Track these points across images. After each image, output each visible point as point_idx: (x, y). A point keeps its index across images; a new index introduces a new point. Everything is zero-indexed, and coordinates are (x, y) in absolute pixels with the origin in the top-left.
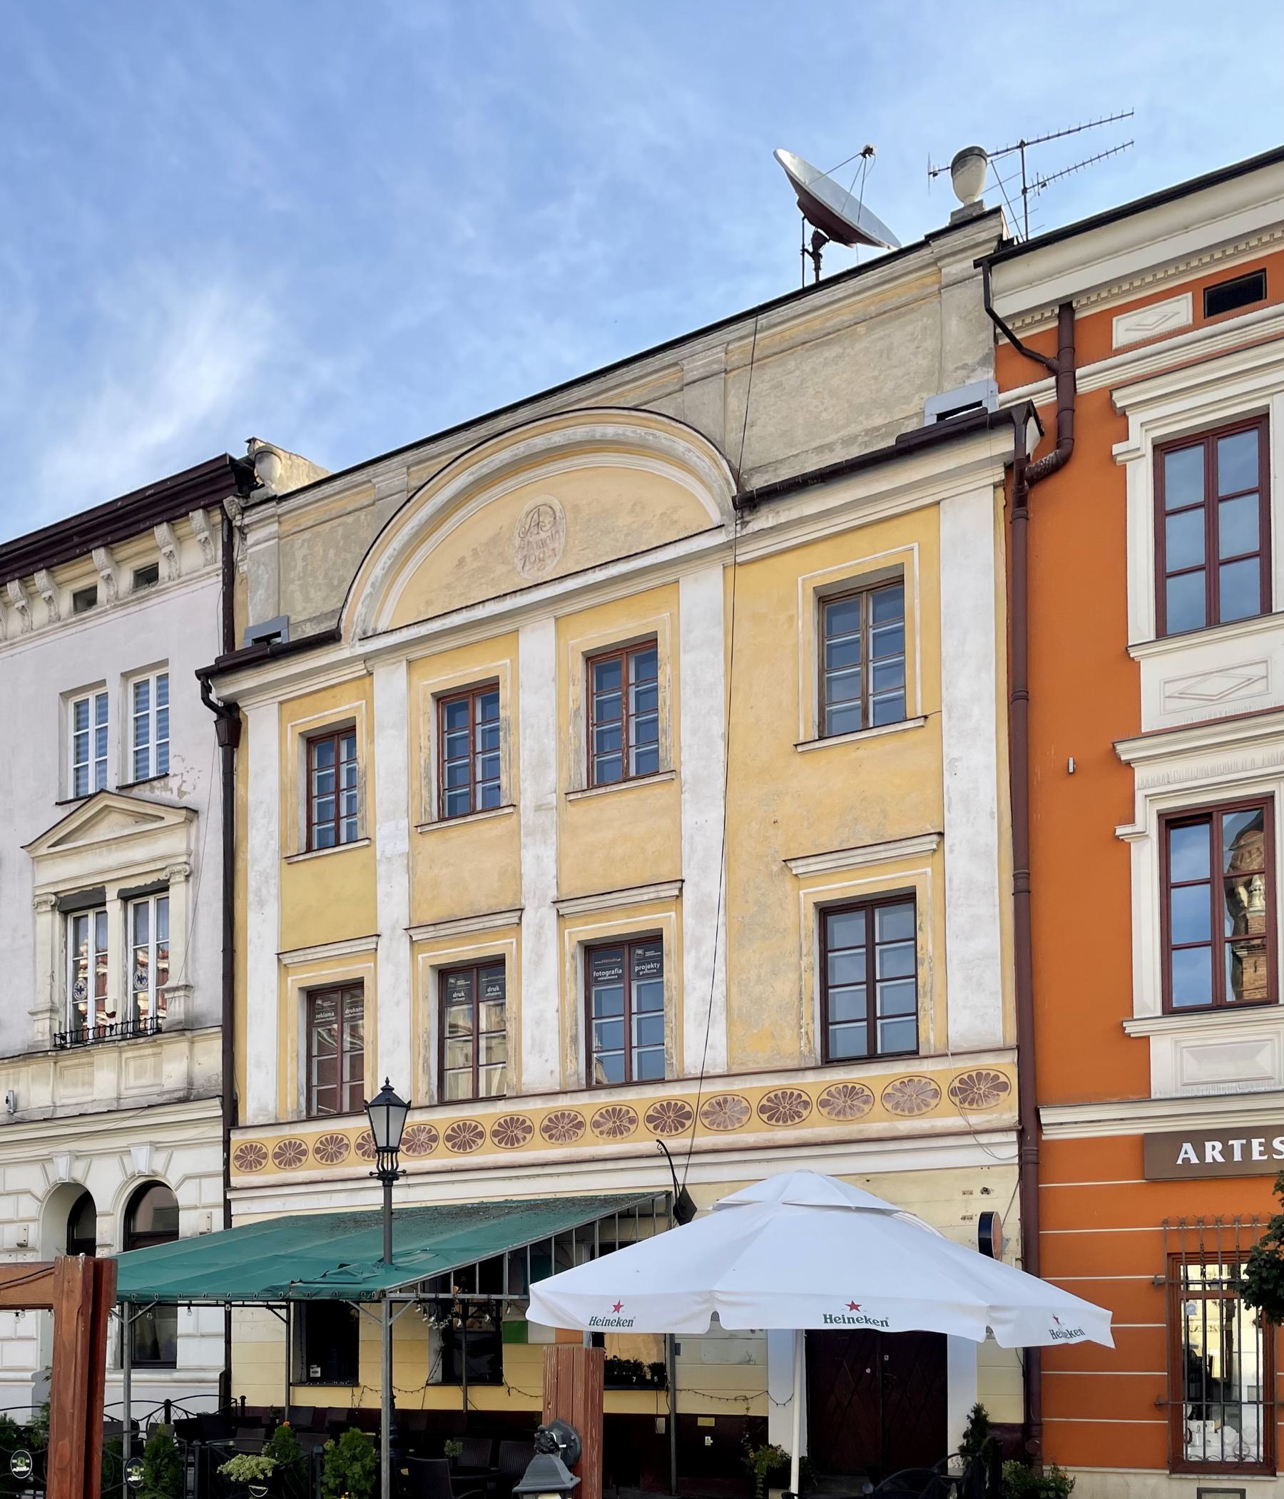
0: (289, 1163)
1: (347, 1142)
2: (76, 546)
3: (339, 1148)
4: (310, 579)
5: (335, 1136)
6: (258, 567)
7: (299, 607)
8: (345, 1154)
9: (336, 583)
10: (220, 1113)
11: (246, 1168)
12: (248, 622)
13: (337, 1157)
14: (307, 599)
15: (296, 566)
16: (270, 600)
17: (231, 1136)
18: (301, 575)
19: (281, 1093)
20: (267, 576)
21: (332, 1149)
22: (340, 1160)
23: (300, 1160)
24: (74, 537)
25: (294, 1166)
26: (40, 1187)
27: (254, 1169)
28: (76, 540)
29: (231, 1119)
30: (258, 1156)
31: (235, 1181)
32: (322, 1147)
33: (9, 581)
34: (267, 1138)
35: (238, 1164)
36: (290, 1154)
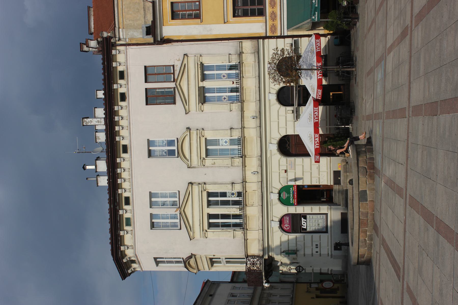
3: (273, 1)
6: (128, 35)
9: (137, 10)
10: (262, 40)
11: (276, 30)
12: (141, 37)
13: (275, 2)
18: (133, 21)
19: (259, 22)
20: (131, 32)
21: (273, 3)
23: (275, 13)
27: (276, 28)
29: (264, 38)
31: (279, 34)
32: (272, 6)
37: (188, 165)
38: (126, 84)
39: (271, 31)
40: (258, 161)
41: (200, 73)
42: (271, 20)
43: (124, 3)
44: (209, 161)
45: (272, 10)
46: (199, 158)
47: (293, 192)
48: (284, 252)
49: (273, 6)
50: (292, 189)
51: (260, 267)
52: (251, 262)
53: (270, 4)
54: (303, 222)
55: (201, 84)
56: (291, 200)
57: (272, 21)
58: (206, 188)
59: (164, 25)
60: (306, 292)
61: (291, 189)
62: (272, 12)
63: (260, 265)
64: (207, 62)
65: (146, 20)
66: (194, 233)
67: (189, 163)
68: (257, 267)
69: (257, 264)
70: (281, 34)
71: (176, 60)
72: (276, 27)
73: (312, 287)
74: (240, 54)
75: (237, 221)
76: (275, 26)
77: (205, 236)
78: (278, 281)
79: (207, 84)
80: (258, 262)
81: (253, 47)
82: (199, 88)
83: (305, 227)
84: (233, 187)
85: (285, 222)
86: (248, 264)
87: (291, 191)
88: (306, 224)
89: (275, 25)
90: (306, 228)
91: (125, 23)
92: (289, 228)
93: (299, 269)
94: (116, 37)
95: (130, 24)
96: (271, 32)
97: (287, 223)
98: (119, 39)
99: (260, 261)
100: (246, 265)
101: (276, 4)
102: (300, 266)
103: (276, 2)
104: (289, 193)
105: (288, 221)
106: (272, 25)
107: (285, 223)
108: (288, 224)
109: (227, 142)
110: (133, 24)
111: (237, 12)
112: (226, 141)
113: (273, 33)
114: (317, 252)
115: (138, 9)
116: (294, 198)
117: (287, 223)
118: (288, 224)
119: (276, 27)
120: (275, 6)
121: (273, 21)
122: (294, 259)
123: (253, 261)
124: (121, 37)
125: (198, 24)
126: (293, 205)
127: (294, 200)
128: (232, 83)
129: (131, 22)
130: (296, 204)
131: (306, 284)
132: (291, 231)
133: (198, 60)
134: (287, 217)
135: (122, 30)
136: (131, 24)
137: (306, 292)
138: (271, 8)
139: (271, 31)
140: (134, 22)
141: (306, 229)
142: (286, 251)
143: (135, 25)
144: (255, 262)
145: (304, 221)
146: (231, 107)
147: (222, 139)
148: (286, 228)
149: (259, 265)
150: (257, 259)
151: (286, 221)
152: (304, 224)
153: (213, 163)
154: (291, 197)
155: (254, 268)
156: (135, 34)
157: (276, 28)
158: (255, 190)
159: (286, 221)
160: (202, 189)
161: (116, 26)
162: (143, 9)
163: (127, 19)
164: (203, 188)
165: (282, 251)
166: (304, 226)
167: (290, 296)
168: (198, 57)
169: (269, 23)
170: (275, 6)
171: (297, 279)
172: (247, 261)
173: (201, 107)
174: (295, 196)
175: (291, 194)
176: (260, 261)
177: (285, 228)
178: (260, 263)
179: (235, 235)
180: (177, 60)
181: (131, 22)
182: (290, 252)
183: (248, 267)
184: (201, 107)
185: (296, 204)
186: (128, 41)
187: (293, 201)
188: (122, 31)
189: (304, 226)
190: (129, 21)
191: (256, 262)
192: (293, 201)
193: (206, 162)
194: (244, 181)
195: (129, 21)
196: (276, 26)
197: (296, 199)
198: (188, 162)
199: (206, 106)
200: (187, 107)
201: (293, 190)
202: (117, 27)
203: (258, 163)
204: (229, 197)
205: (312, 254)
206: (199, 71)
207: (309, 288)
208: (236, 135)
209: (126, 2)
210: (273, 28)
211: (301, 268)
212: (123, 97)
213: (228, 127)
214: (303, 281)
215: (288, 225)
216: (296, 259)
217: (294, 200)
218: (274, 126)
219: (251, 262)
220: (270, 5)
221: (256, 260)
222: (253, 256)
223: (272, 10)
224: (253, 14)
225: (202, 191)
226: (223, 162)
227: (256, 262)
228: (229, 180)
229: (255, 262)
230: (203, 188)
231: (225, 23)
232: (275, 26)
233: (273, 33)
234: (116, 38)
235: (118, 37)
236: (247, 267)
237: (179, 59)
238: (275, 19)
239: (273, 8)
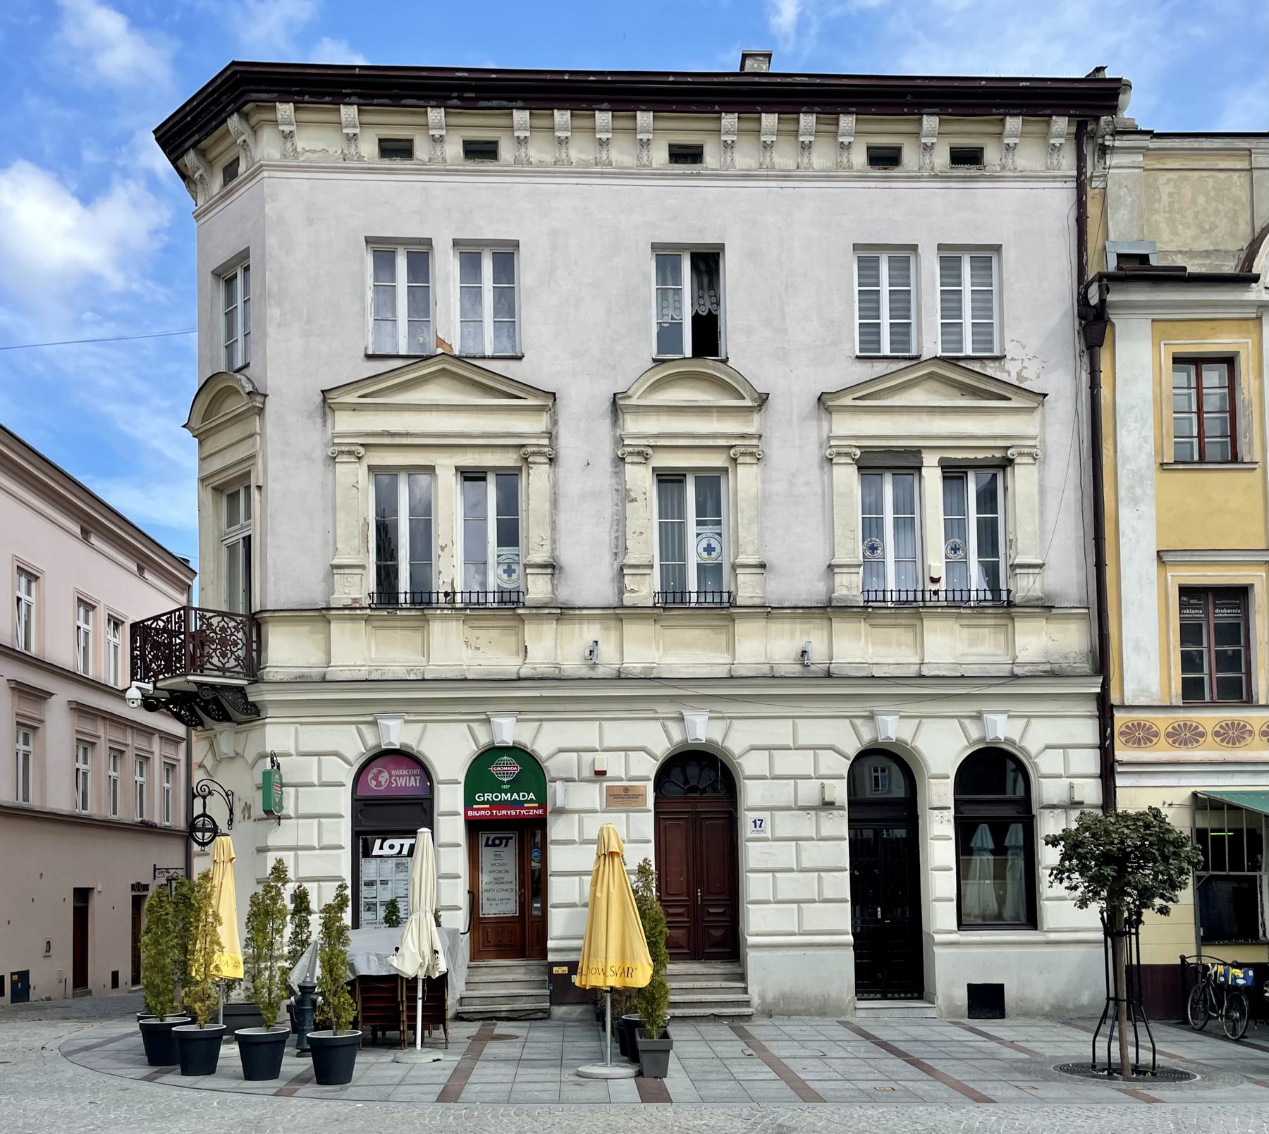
0: (1185, 743)
1: (1251, 729)
2: (906, 105)
4: (1177, 216)
5: (1236, 722)
7: (1166, 236)
8: (1249, 739)
9: (1207, 227)
11: (1134, 743)
13: (1239, 741)
14: (1174, 232)
15: (1161, 198)
16: (1135, 223)
17: (1115, 713)
18: (1167, 209)
20: (1130, 199)
21: (1233, 733)
22: (1243, 744)
23: (1197, 741)
24: (910, 96)
25: (1190, 746)
26: (853, 747)
27: (1143, 745)
28: (909, 98)
30: (1148, 734)
32: (1222, 731)
33: (804, 113)
34: (1157, 718)
35: (1124, 740)
36: (1186, 735)
37: (625, 395)
38: (933, 169)
39: (1133, 724)
40: (643, 667)
41: (971, 455)
42: (1173, 728)
43: (1235, 175)
44: (641, 478)
45: (1209, 731)
46: (652, 442)
47: (518, 804)
48: (272, 767)
49: (1225, 734)
50: (531, 801)
53: (1229, 723)
54: (397, 842)
55: (930, 461)
56: (488, 796)
57: (1170, 729)
58: (534, 463)
59: (1154, 323)
61: (532, 796)
62: (1201, 729)
63: (218, 669)
64: (1022, 480)
65: (1174, 257)
66: (354, 408)
67: (634, 401)
69: (224, 655)
70: (1122, 764)
71: (1025, 367)
72: (1146, 743)
74: (1045, 607)
75: (404, 584)
76: (1151, 741)
77: (342, 452)
79: (932, 478)
80: (232, 663)
81: (1066, 658)
82: (917, 452)
83: (376, 851)
84: (540, 571)
85: (400, 772)
87: (524, 796)
88: (392, 856)
89: (1155, 740)
90: (374, 853)
91: (1163, 177)
92: (373, 786)
93: (204, 830)
94: (1117, 137)
95: (1157, 196)
96: (1127, 727)
97: (395, 780)
98: (1104, 150)
100: (220, 613)
101: (1230, 745)
103: (1237, 745)
104: (516, 785)
105: (402, 782)
106: (1155, 729)
107: (393, 772)
108: (391, 783)
109: (709, 554)
110: (1156, 205)
111: (1192, 601)
112: (714, 549)
113: (1122, 733)
115: (1211, 230)
116: (494, 805)
117: (395, 780)
118: (391, 783)
119: (1146, 743)
120: (1222, 741)
121: (1168, 735)
122: (247, 808)
123: (236, 644)
124: (1113, 160)
125: (1160, 451)
126: (469, 802)
127: (488, 806)
128: (936, 576)
129: (1165, 199)
130: (470, 813)
132: (362, 793)
133: (1022, 450)
134: (418, 778)
135: (1140, 162)
136: (1159, 201)
138: (1218, 728)
139: (1133, 724)
140: (1164, 212)
141: (367, 853)
142: (281, 776)
143: (1155, 217)
144: (231, 651)
145: (402, 846)
146: (845, 570)
147: (720, 535)
148: (376, 778)
149: (220, 665)
151: (403, 776)
152: (392, 847)
153: (633, 495)
154: (497, 797)
156: (1122, 212)
157: (1143, 745)
158: (529, 655)
159: (403, 776)
160: (530, 449)
161: (1155, 140)
162: (1211, 248)
163: (1175, 186)
164: (534, 454)
165: (280, 760)
166: (381, 848)
168: (1035, 450)
169: (1162, 721)
170: (1224, 744)
172: (239, 619)
173: (847, 454)
174: (504, 812)
175: (509, 794)
177: (375, 771)
178: (228, 670)
179: (347, 571)
180: (1021, 371)
181: (1165, 199)
182: (276, 789)
184: (847, 454)
185: (470, 813)
186: (1094, 185)
187: (483, 803)
188: (1134, 162)
189: (381, 848)
190: (1171, 195)
191: (232, 653)
192: (483, 803)
193: (636, 467)
194: (563, 612)
195: (1171, 195)
196: (1149, 744)
197: (492, 813)
198: (637, 396)
199: (847, 477)
200: (847, 401)
201: (527, 802)
202: (1151, 145)
203: (634, 668)
204: (499, 556)
206: (981, 455)
208: (747, 589)
209: (1238, 184)
210: (1144, 735)
211: (207, 835)
212: (884, 158)
213: (770, 557)
214: (1107, 1054)
215: (384, 785)
216: (246, 816)
217: (488, 806)
218: (778, 732)
219: (232, 634)
220: (1227, 724)
222: (256, 644)
223: (1209, 731)
224: (1190, 662)
225: (524, 450)
226: (637, 533)
227: (232, 653)
228: (567, 556)
229: (231, 651)
230: (534, 454)
231: (1158, 552)
232: (1151, 741)
233: (1122, 733)
234: (1112, 135)
235: (1117, 144)
237: (1026, 379)
238: (1174, 742)
239: (1217, 734)
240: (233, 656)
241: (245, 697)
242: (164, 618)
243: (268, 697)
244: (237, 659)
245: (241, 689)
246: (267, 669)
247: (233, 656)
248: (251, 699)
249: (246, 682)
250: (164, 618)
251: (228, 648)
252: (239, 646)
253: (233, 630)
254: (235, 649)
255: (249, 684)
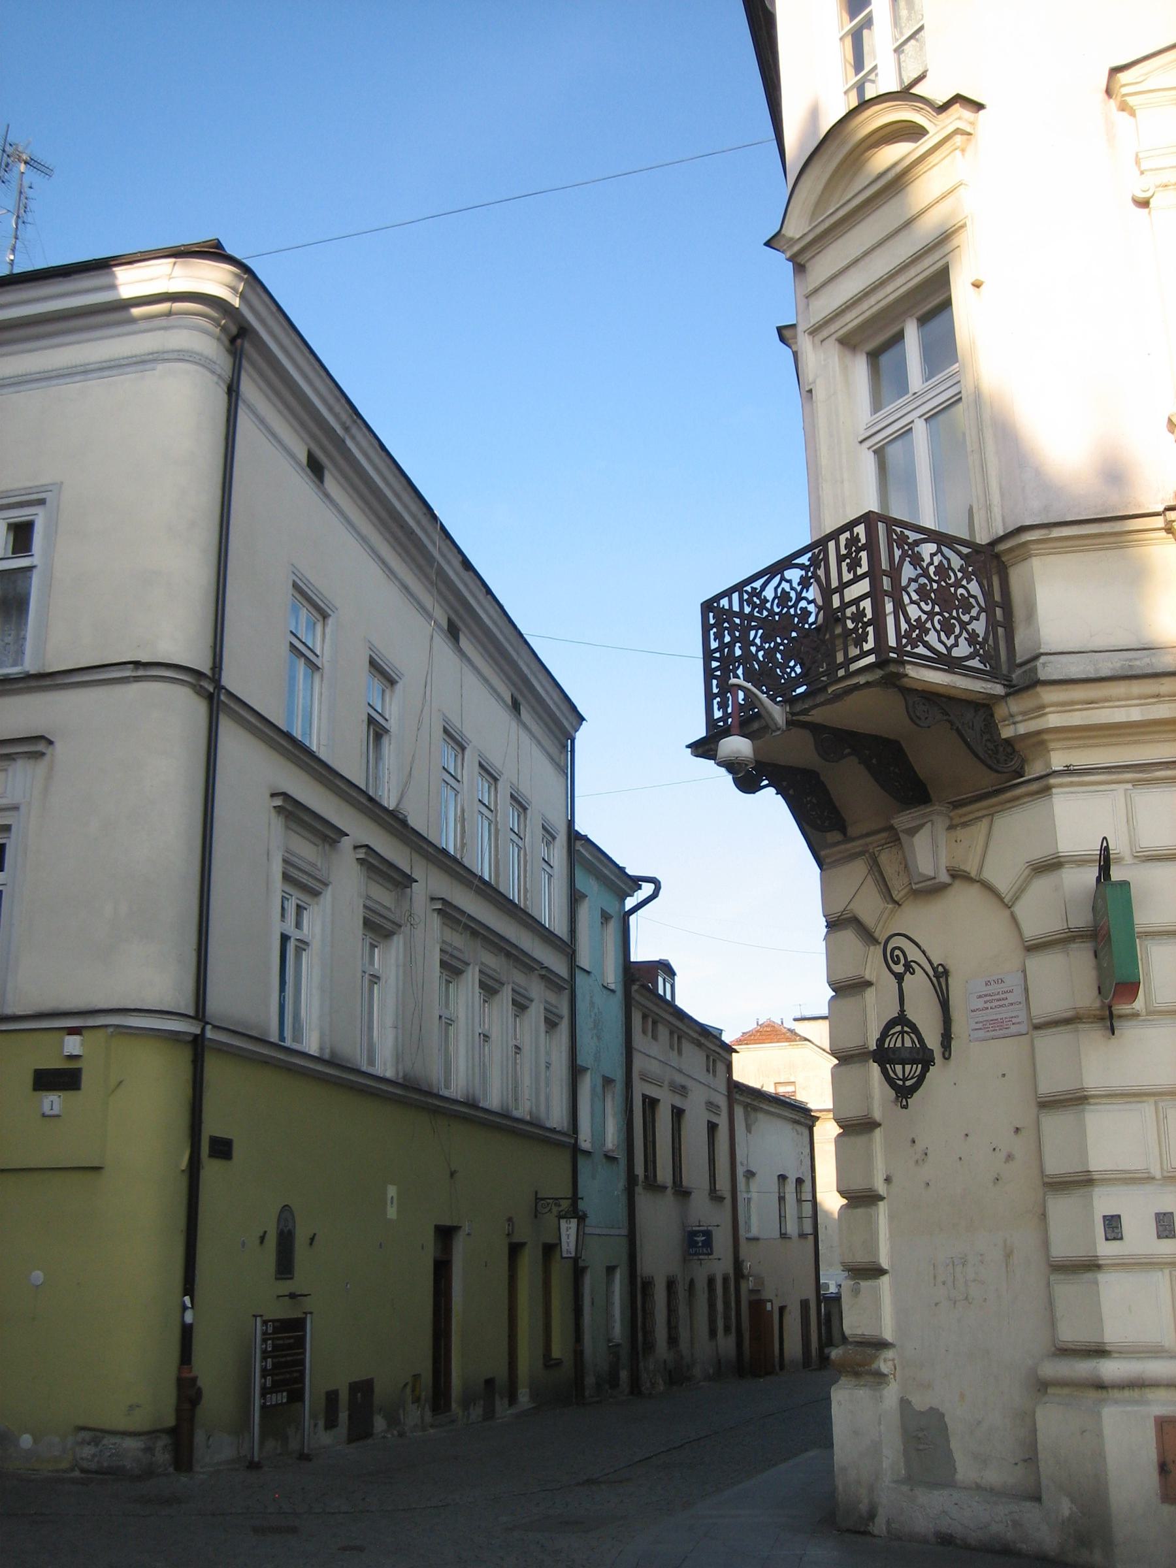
51: (921, 650)
52: (957, 584)
60: (536, 1193)
68: (927, 631)
73: (563, 1222)
78: (579, 1062)
86: (939, 551)
99: (969, 663)
102: (924, 1059)
114: (1113, 1225)
131: (565, 1191)
137: (536, 1193)
150: (986, 639)
155: (915, 597)
167: (516, 1109)
171: (587, 1153)
176: (969, 663)
183: (917, 543)
205: (1084, 1181)
207: (555, 1210)
219: (957, 584)
221: (979, 627)
227: (964, 626)
236: (913, 536)
240: (965, 634)
241: (990, 726)
242: (804, 560)
243: (1054, 720)
244: (972, 639)
245: (983, 707)
246: (1042, 659)
247: (965, 634)
248: (1007, 732)
249: (998, 689)
250: (804, 560)
251: (954, 614)
252: (974, 612)
253: (960, 575)
254: (966, 618)
255: (1008, 695)
